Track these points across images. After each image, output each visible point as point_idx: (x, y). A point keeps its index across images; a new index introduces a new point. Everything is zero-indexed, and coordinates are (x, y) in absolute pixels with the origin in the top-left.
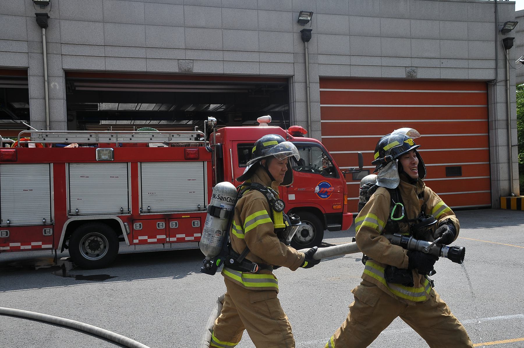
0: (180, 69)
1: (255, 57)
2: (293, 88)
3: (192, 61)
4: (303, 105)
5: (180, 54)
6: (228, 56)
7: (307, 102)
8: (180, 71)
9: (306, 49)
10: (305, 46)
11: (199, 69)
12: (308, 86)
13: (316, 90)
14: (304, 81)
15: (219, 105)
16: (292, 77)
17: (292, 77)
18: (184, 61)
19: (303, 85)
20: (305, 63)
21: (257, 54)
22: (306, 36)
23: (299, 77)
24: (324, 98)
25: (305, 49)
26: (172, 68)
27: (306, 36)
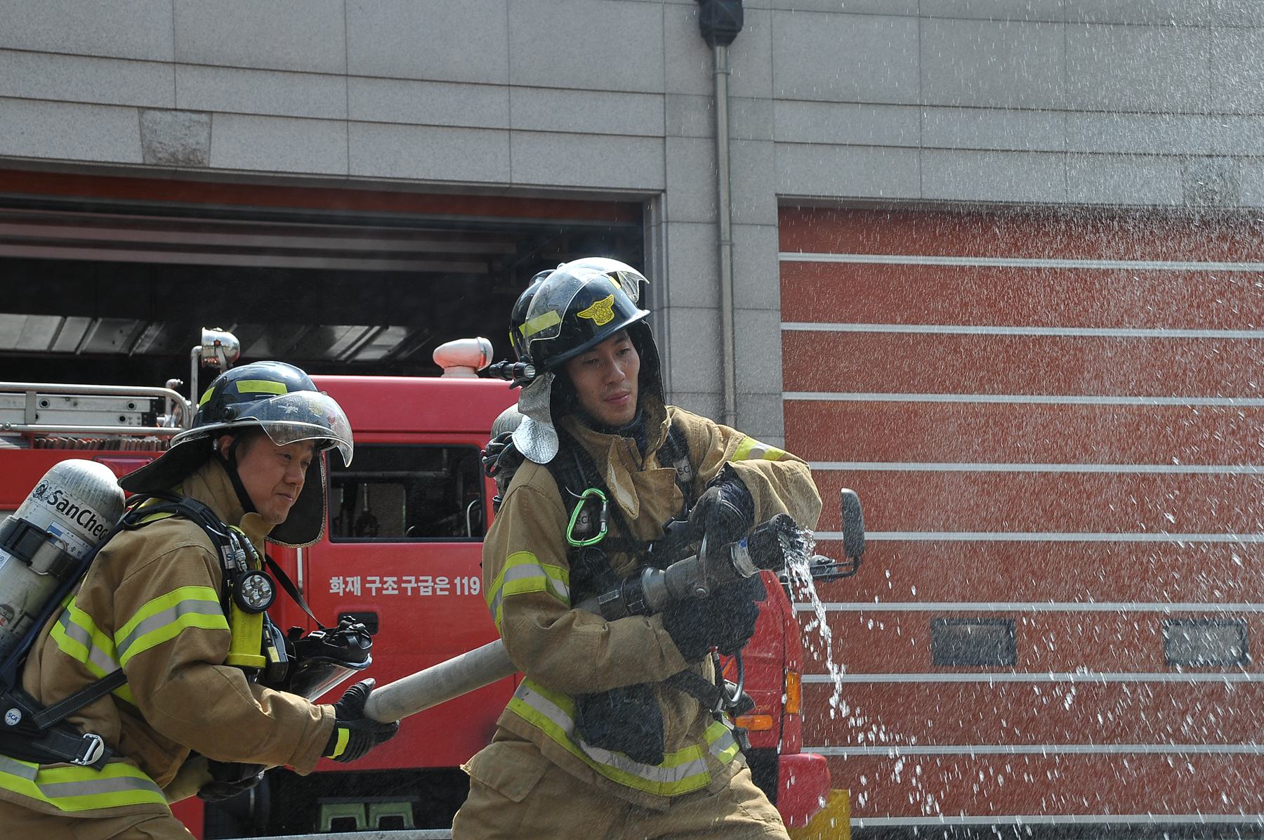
0: (147, 148)
1: (492, 106)
2: (659, 246)
3: (204, 118)
4: (705, 320)
5: (151, 87)
6: (369, 101)
7: (719, 308)
8: (150, 160)
9: (721, 79)
10: (714, 65)
11: (234, 152)
12: (725, 236)
13: (761, 257)
14: (709, 216)
15: (359, 330)
16: (655, 197)
17: (655, 197)
18: (168, 117)
19: (705, 232)
20: (714, 137)
21: (500, 96)
22: (718, 19)
23: (684, 199)
24: (799, 291)
25: (714, 79)
26: (113, 144)
27: (718, 19)
